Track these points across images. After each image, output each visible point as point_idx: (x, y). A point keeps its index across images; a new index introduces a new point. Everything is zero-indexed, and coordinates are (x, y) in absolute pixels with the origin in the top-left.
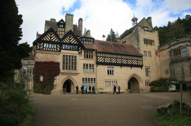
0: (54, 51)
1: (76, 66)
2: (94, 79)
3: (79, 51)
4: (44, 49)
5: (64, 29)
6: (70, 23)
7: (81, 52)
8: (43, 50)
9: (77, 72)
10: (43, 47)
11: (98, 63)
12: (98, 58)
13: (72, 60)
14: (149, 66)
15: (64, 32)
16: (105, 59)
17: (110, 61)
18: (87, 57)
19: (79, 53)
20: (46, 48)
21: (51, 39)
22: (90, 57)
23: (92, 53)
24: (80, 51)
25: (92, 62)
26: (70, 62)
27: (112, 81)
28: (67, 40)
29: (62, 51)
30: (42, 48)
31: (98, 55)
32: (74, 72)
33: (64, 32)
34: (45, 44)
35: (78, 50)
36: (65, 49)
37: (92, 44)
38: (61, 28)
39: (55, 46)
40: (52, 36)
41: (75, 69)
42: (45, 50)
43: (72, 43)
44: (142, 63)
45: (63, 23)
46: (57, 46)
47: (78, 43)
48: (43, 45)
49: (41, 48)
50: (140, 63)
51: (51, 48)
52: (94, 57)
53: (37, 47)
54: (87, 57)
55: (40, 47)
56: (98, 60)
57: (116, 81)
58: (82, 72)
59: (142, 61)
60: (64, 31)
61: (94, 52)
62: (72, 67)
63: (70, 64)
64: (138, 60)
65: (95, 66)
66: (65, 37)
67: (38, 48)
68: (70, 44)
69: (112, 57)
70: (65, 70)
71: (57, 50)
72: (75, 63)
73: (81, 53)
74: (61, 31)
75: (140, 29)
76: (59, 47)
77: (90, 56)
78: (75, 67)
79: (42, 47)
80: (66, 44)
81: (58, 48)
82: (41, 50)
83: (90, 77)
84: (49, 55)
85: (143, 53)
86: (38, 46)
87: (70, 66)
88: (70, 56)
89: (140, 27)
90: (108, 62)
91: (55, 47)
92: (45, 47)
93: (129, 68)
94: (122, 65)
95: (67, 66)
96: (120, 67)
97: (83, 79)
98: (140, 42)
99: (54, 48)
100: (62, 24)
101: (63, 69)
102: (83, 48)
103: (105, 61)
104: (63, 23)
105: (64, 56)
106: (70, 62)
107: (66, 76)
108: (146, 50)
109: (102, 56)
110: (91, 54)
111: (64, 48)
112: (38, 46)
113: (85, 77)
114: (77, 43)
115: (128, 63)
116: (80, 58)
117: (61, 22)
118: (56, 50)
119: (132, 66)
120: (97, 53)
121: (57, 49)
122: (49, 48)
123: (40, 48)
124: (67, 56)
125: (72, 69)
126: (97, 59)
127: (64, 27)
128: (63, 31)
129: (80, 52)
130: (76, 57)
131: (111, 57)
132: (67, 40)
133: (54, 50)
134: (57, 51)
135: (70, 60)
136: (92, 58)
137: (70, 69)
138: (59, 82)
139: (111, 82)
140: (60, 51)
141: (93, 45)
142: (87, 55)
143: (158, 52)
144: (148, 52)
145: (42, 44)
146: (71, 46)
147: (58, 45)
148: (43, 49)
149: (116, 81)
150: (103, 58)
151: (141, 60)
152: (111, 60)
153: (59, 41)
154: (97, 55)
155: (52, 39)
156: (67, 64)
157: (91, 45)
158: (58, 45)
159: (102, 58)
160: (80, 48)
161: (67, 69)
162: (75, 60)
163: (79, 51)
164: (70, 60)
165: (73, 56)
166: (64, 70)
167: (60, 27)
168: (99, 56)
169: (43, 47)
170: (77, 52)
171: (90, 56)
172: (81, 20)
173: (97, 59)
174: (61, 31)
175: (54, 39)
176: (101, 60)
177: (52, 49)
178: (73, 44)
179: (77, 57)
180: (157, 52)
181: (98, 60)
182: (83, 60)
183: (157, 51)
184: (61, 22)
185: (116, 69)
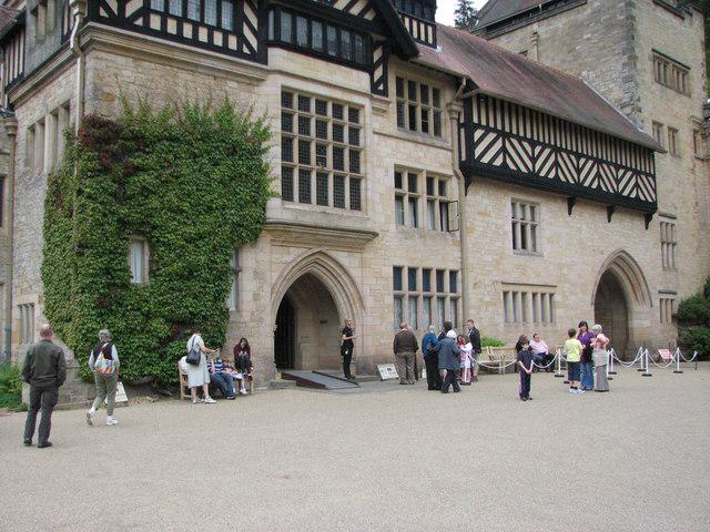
0: (225, 49)
2: (453, 274)
7: (384, 79)
8: (146, 29)
9: (369, 226)
11: (473, 172)
14: (673, 213)
18: (414, 122)
23: (436, 103)
24: (378, 73)
25: (437, 158)
27: (535, 289)
30: (136, 15)
31: (475, 120)
35: (368, 68)
36: (293, 47)
44: (655, 191)
52: (449, 130)
57: (548, 291)
58: (393, 227)
63: (322, 160)
65: (454, 188)
70: (296, 205)
76: (254, 22)
82: (127, 23)
83: (434, 265)
84: (189, 77)
85: (648, 130)
88: (321, 105)
90: (524, 170)
97: (397, 270)
101: (287, 195)
103: (509, 161)
105: (287, 96)
108: (661, 119)
113: (406, 264)
121: (242, 40)
123: (122, 8)
126: (471, 146)
129: (379, 82)
130: (355, 112)
134: (238, 53)
138: (256, 297)
139: (530, 296)
140: (260, 57)
144: (670, 129)
147: (248, 12)
148: (147, 22)
149: (552, 290)
150: (499, 145)
154: (469, 116)
158: (248, 12)
160: (377, 55)
161: (305, 198)
166: (288, 205)
176: (488, 151)
181: (478, 152)
182: (393, 142)
185: (552, 218)
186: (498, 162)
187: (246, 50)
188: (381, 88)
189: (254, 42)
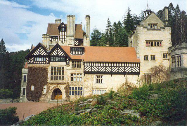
0: (44, 64)
1: (63, 76)
3: (66, 62)
4: (35, 62)
5: (65, 32)
6: (72, 25)
7: (69, 62)
8: (34, 63)
10: (34, 61)
11: (85, 73)
12: (85, 67)
13: (60, 71)
15: (66, 35)
16: (92, 68)
17: (98, 70)
19: (67, 64)
20: (36, 62)
21: (40, 53)
22: (78, 67)
23: (80, 63)
26: (58, 73)
28: (54, 53)
29: (51, 63)
30: (32, 62)
31: (85, 65)
32: (61, 81)
33: (65, 36)
34: (36, 59)
35: (66, 61)
36: (54, 62)
37: (81, 54)
38: (63, 31)
39: (45, 59)
40: (41, 50)
41: (63, 79)
42: (36, 63)
43: (60, 55)
45: (64, 26)
46: (46, 59)
47: (65, 55)
48: (34, 59)
49: (32, 62)
50: (135, 70)
51: (39, 61)
52: (82, 67)
53: (28, 62)
54: (75, 67)
55: (31, 61)
56: (85, 70)
59: (139, 67)
60: (65, 34)
61: (82, 62)
62: (60, 77)
64: (119, 67)
65: (83, 75)
66: (53, 50)
67: (29, 62)
68: (58, 56)
69: (101, 66)
71: (46, 63)
72: (63, 74)
73: (69, 64)
74: (64, 35)
75: (142, 29)
76: (48, 59)
77: (78, 65)
78: (63, 77)
79: (33, 61)
80: (54, 56)
81: (47, 61)
86: (29, 61)
87: (57, 77)
89: (142, 27)
90: (96, 71)
91: (45, 60)
92: (36, 60)
93: (122, 76)
94: (112, 73)
95: (55, 77)
96: (111, 75)
98: (139, 45)
99: (41, 61)
100: (63, 27)
101: (52, 79)
102: (70, 59)
104: (64, 26)
105: (52, 67)
106: (58, 73)
107: (55, 85)
109: (90, 66)
110: (79, 64)
111: (52, 61)
112: (29, 61)
114: (64, 55)
115: (119, 71)
116: (68, 68)
117: (62, 26)
118: (45, 63)
119: (124, 73)
120: (84, 63)
121: (46, 62)
122: (37, 61)
124: (55, 67)
125: (60, 79)
127: (65, 30)
128: (64, 35)
130: (63, 68)
131: (100, 65)
132: (54, 53)
133: (44, 63)
134: (46, 64)
135: (58, 71)
136: (80, 67)
137: (57, 79)
140: (49, 63)
141: (82, 54)
142: (75, 65)
143: (168, 55)
145: (33, 58)
146: (59, 58)
147: (47, 58)
148: (34, 63)
151: (120, 66)
152: (112, 69)
153: (47, 55)
155: (41, 53)
156: (55, 74)
157: (80, 54)
159: (89, 67)
160: (67, 59)
161: (55, 79)
162: (63, 71)
163: (66, 62)
164: (58, 71)
165: (60, 68)
167: (61, 31)
168: (86, 66)
169: (33, 62)
170: (65, 63)
171: (78, 65)
172: (88, 17)
173: (84, 69)
174: (63, 35)
175: (43, 53)
176: (88, 69)
177: (42, 62)
178: (61, 56)
179: (65, 68)
180: (166, 55)
181: (85, 70)
183: (166, 53)
184: (62, 26)
186: (91, 70)
187: (47, 63)
188: (68, 63)
189: (48, 62)
